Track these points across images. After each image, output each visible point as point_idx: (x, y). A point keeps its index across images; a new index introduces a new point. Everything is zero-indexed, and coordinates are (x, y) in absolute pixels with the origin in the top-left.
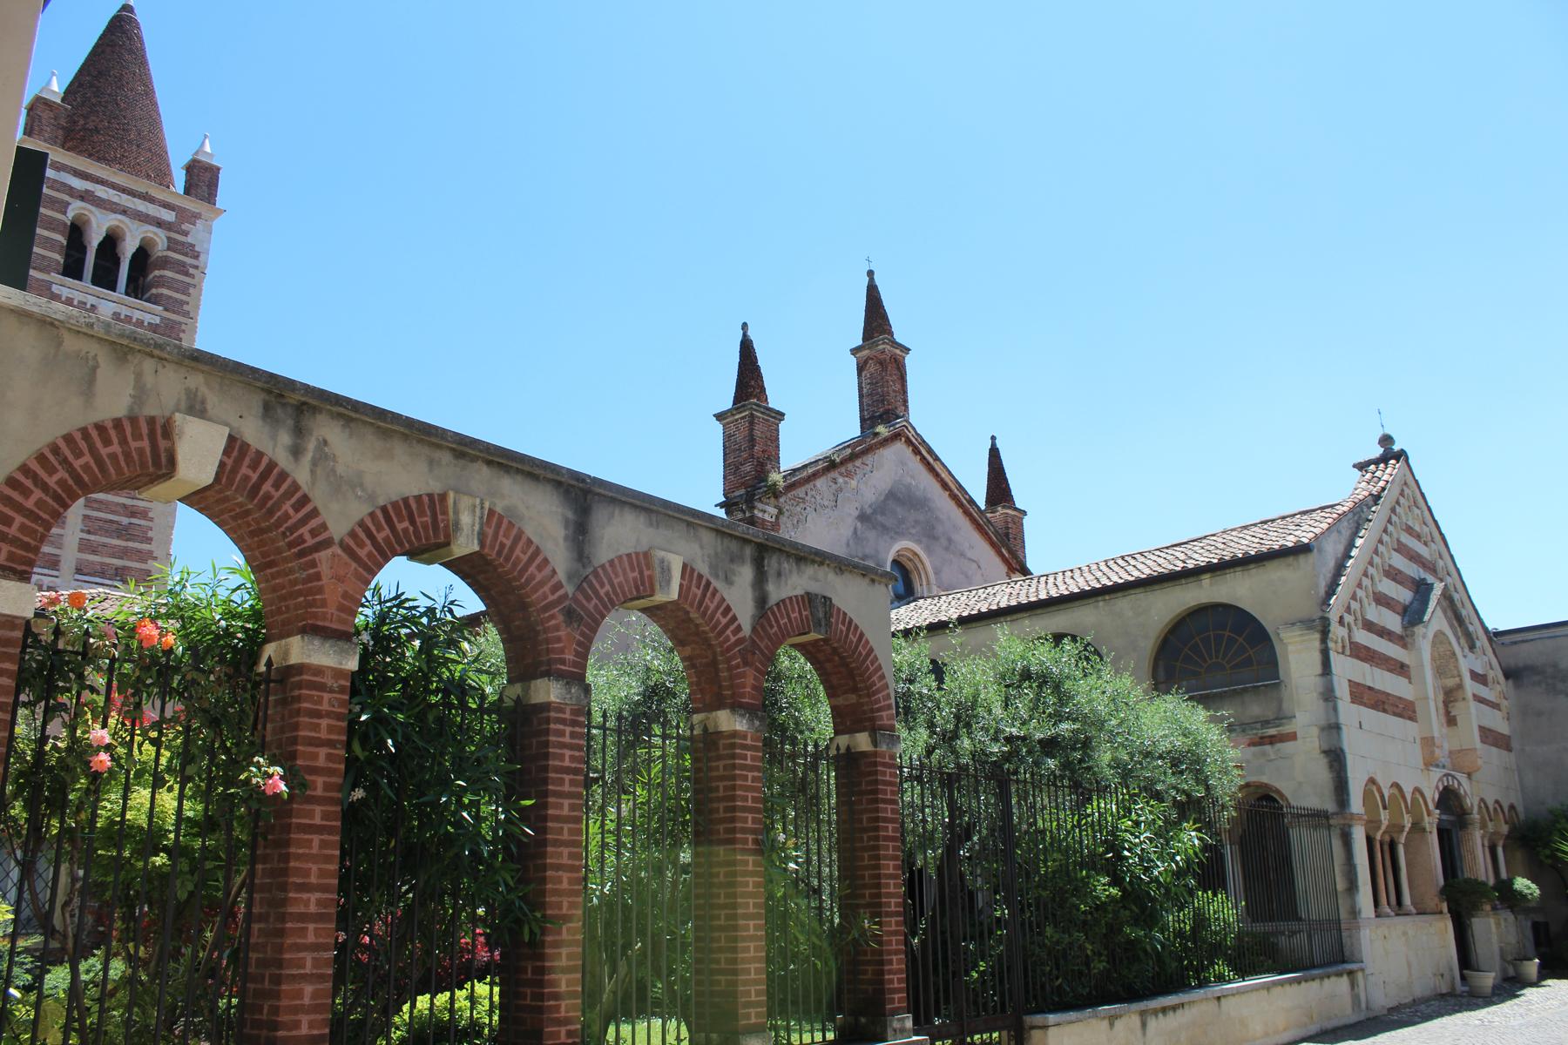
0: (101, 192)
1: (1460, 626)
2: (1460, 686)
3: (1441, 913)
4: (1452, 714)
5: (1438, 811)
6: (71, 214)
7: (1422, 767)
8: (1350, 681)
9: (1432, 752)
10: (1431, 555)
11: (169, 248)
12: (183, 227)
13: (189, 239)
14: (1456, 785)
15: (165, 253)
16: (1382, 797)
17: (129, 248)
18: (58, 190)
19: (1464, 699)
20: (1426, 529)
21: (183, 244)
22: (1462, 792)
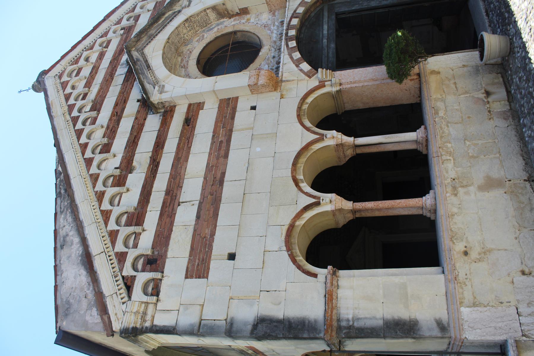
1: (164, 14)
2: (214, 8)
3: (419, 75)
5: (320, 70)
7: (277, 94)
8: (186, 277)
9: (263, 86)
10: (116, 37)
14: (295, 22)
19: (224, 4)
20: (97, 47)
22: (301, 10)
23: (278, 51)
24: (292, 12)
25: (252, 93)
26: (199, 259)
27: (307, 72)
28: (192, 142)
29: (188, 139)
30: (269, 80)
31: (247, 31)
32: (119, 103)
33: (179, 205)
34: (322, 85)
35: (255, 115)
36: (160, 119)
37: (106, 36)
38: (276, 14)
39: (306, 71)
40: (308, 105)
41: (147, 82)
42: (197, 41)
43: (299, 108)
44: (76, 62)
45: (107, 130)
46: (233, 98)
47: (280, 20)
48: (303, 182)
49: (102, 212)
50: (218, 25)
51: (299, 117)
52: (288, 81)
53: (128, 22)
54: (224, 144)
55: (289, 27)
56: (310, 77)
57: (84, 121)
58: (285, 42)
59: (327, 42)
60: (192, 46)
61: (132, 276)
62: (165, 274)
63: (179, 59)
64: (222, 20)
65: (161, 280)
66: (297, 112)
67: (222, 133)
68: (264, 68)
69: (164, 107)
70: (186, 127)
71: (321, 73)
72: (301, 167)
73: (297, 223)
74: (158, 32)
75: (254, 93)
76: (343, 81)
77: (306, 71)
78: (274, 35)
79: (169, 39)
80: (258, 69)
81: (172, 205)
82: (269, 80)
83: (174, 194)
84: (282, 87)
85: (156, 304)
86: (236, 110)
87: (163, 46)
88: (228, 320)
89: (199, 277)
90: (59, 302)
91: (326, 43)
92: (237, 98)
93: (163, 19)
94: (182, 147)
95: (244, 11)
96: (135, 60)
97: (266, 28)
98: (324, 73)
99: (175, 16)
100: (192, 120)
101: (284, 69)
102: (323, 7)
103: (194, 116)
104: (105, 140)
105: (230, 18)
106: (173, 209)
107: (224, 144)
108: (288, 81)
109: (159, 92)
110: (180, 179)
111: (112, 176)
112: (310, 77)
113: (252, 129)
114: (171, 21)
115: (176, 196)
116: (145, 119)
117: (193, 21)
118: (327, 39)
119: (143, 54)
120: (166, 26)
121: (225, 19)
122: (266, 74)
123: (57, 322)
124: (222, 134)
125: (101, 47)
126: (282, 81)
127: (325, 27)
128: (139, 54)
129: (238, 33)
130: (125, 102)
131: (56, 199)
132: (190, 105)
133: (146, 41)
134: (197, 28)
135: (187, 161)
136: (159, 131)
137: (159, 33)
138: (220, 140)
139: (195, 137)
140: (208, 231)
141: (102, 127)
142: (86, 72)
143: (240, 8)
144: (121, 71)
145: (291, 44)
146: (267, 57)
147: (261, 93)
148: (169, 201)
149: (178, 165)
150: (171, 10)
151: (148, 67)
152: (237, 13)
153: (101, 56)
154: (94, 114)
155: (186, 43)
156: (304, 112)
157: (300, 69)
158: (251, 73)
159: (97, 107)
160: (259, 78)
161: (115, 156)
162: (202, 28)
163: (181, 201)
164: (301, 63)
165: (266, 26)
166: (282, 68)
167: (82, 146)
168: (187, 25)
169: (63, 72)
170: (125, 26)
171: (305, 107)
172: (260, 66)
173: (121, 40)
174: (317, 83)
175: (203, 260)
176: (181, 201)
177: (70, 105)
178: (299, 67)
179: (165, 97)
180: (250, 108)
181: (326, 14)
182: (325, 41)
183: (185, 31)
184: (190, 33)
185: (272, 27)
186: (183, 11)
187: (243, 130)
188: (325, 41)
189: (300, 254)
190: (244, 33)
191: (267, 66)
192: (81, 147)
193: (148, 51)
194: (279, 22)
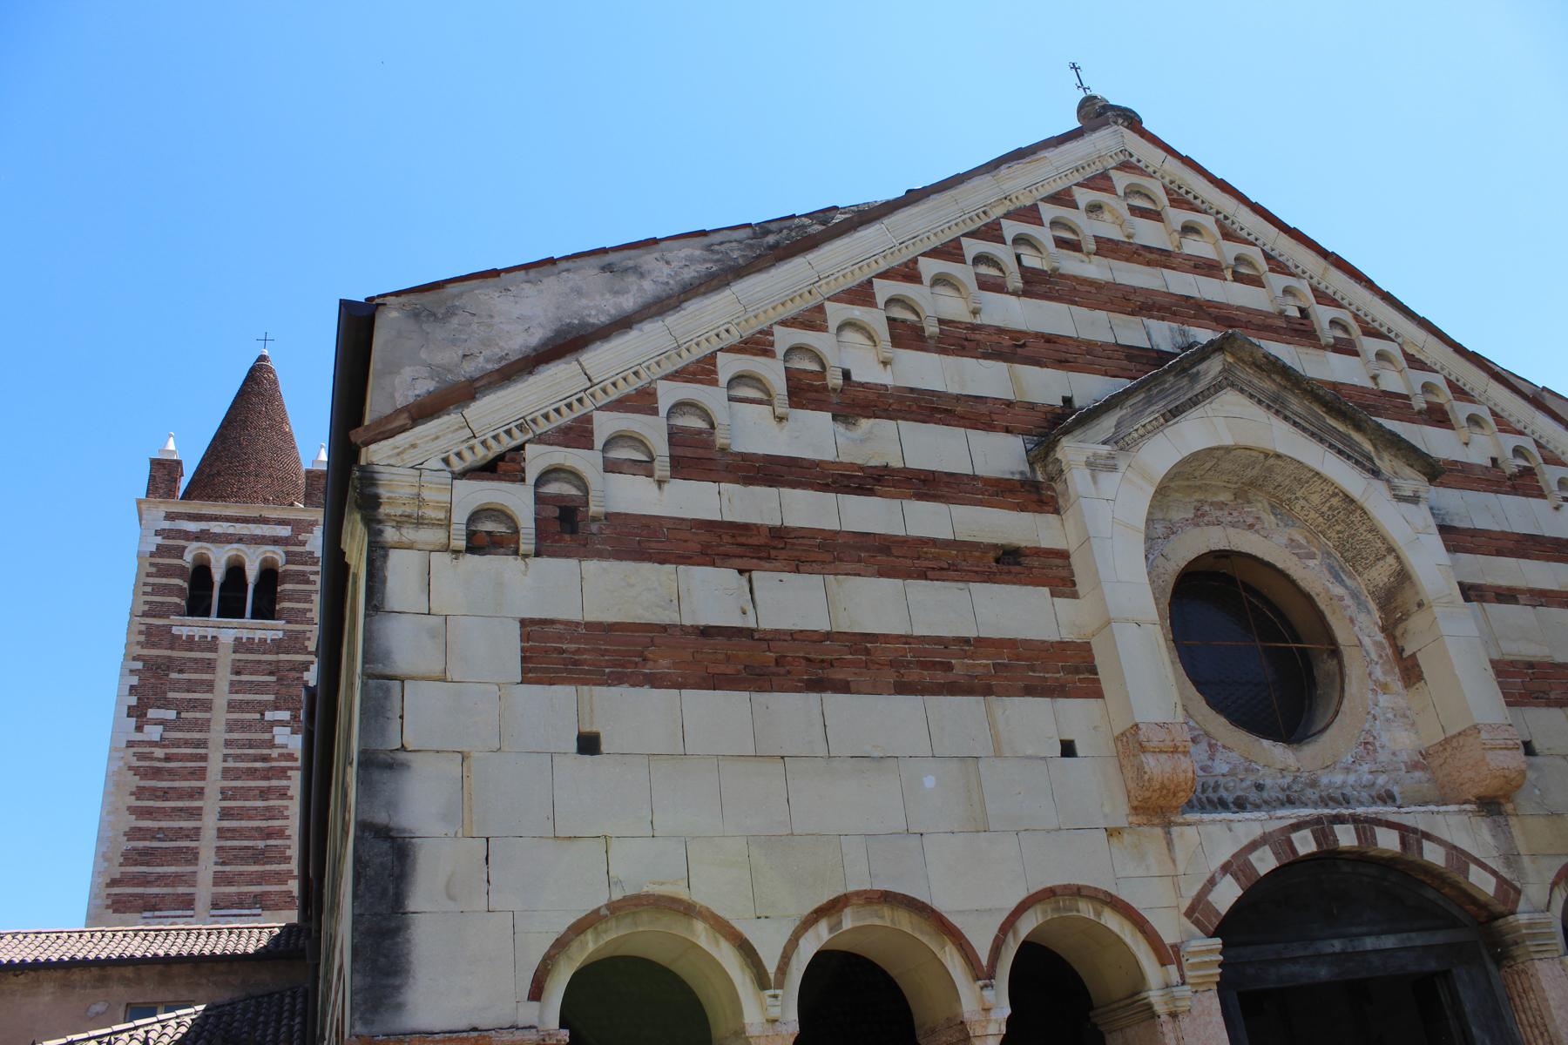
0: (216, 527)
1: (1358, 427)
2: (1403, 576)
4: (1406, 654)
5: (1217, 943)
6: (189, 557)
7: (1120, 814)
9: (1140, 770)
11: (287, 562)
12: (300, 538)
13: (308, 548)
14: (1388, 841)
15: (284, 568)
16: (746, 950)
17: (252, 573)
18: (174, 538)
19: (1420, 605)
20: (1231, 250)
21: (301, 554)
22: (1433, 855)
23: (1282, 796)
24: (1422, 827)
25: (1116, 739)
26: (578, 651)
27: (1209, 904)
28: (944, 580)
29: (953, 567)
30: (1163, 786)
31: (1342, 689)
32: (1057, 346)
33: (741, 572)
34: (1167, 954)
35: (1042, 758)
36: (1013, 473)
37: (1271, 270)
38: (1418, 774)
39: (1212, 897)
40: (1092, 917)
41: (1121, 417)
42: (1292, 540)
43: (1077, 892)
44: (1179, 200)
45: (966, 328)
46: (1098, 681)
47: (1396, 790)
48: (831, 930)
49: (711, 358)
50: (1355, 595)
51: (1049, 894)
52: (1168, 844)
53: (1326, 325)
54: (940, 677)
55: (1364, 826)
56: (1189, 913)
57: (990, 257)
58: (1308, 819)
59: (1334, 954)
60: (1274, 526)
61: (523, 470)
62: (532, 561)
63: (1224, 497)
64: (1373, 606)
65: (516, 552)
66: (1066, 887)
67: (980, 665)
68: (1217, 762)
69: (1052, 479)
70: (992, 555)
71: (1204, 948)
72: (882, 918)
73: (699, 926)
74: (1297, 420)
75: (1119, 744)
76: (1185, 1022)
77: (1212, 897)
78: (1338, 778)
79: (1278, 456)
80: (1214, 742)
81: (740, 550)
82: (1163, 786)
83: (773, 553)
84: (1146, 829)
85: (446, 548)
86: (1059, 697)
87: (1250, 443)
88: (402, 756)
89: (524, 659)
90: (452, 289)
91: (1330, 950)
92: (1097, 693)
93: (1341, 428)
94: (926, 553)
95: (1411, 672)
96: (1195, 370)
97: (1361, 748)
98: (1207, 959)
99: (1357, 462)
100: (1018, 569)
101: (1211, 828)
102: (1467, 926)
103: (1027, 572)
104: (932, 329)
105: (1383, 629)
106: (727, 556)
107: (940, 677)
108: (1170, 844)
109: (1092, 459)
110: (823, 562)
111: (823, 366)
112: (1189, 913)
113: (998, 754)
114: (1340, 452)
115: (769, 558)
116: (1007, 430)
117: (1352, 518)
118: (1343, 952)
119: (1216, 388)
120: (1321, 440)
121: (1376, 614)
122: (1182, 776)
123: (398, 294)
124: (974, 665)
125: (1233, 262)
126: (1167, 825)
127: (1389, 942)
128: (1215, 378)
129: (1335, 662)
130: (1060, 361)
131: (749, 225)
132: (1064, 555)
133: (1262, 391)
134: (1334, 535)
135: (881, 574)
136: (974, 477)
137: (1295, 424)
138: (953, 661)
139: (961, 585)
140: (663, 665)
141: (975, 312)
142: (1148, 234)
143: (1418, 655)
144: (1162, 334)
145: (1305, 838)
146: (1256, 766)
147: (1121, 767)
148: (754, 541)
149: (867, 551)
150: (1375, 446)
151: (1175, 413)
152: (1403, 650)
153: (1208, 268)
154: (1015, 281)
155: (1282, 508)
156: (1066, 909)
157: (1217, 879)
158: (1178, 727)
159: (1037, 284)
160: (1165, 756)
161: (885, 363)
162: (1336, 547)
163: (755, 574)
164: (1237, 879)
165: (1369, 747)
166: (1214, 821)
167: (911, 265)
168: (1335, 501)
169: (1142, 172)
170: (1313, 317)
171: (1086, 910)
172: (1224, 747)
173: (1268, 315)
174: (1169, 937)
175: (576, 663)
176: (755, 574)
177: (1038, 211)
178: (1224, 875)
179: (1078, 479)
180: (1067, 737)
181: (1440, 938)
182: (1338, 945)
183: (1316, 499)
184: (1313, 515)
185: (1366, 768)
186: (1379, 485)
187: (992, 725)
188: (1338, 945)
189: (602, 942)
190: (1338, 679)
191: (1225, 769)
192: (906, 264)
193: (1231, 401)
194: (1389, 787)
